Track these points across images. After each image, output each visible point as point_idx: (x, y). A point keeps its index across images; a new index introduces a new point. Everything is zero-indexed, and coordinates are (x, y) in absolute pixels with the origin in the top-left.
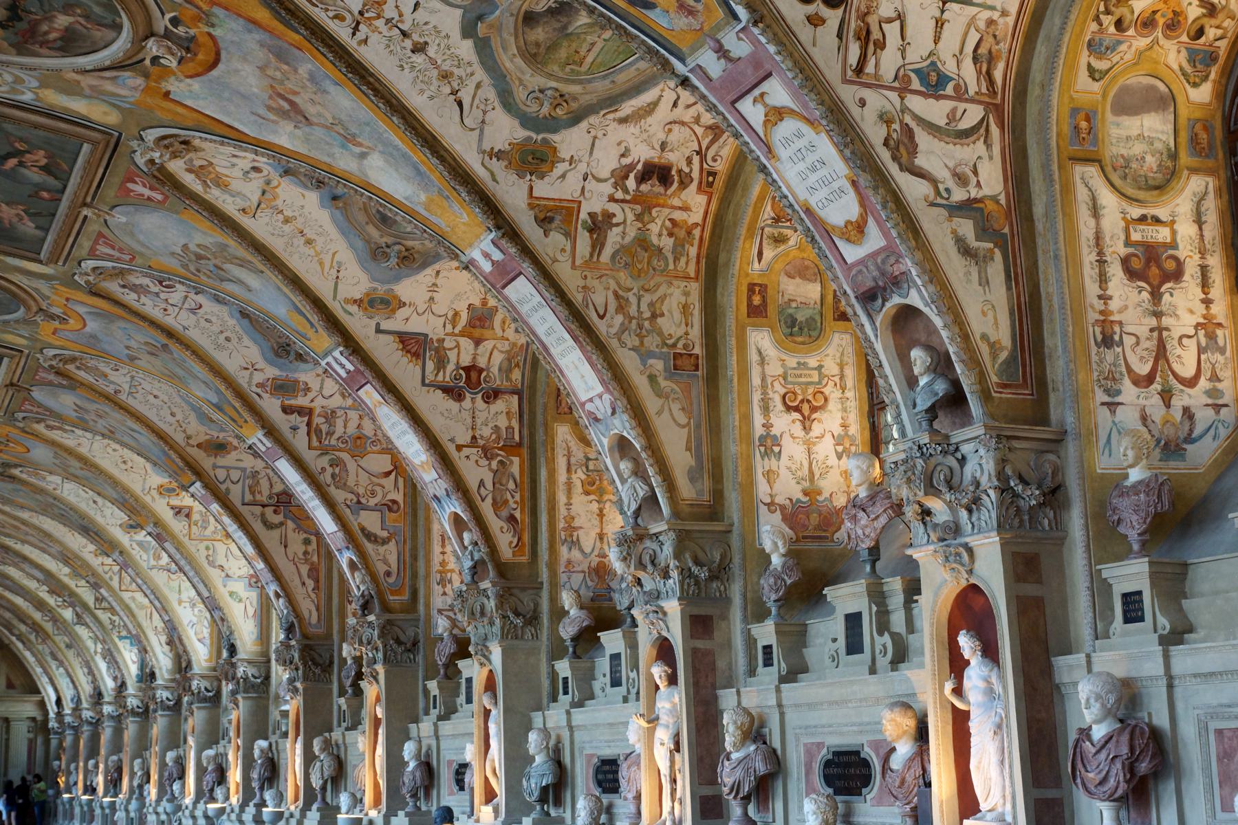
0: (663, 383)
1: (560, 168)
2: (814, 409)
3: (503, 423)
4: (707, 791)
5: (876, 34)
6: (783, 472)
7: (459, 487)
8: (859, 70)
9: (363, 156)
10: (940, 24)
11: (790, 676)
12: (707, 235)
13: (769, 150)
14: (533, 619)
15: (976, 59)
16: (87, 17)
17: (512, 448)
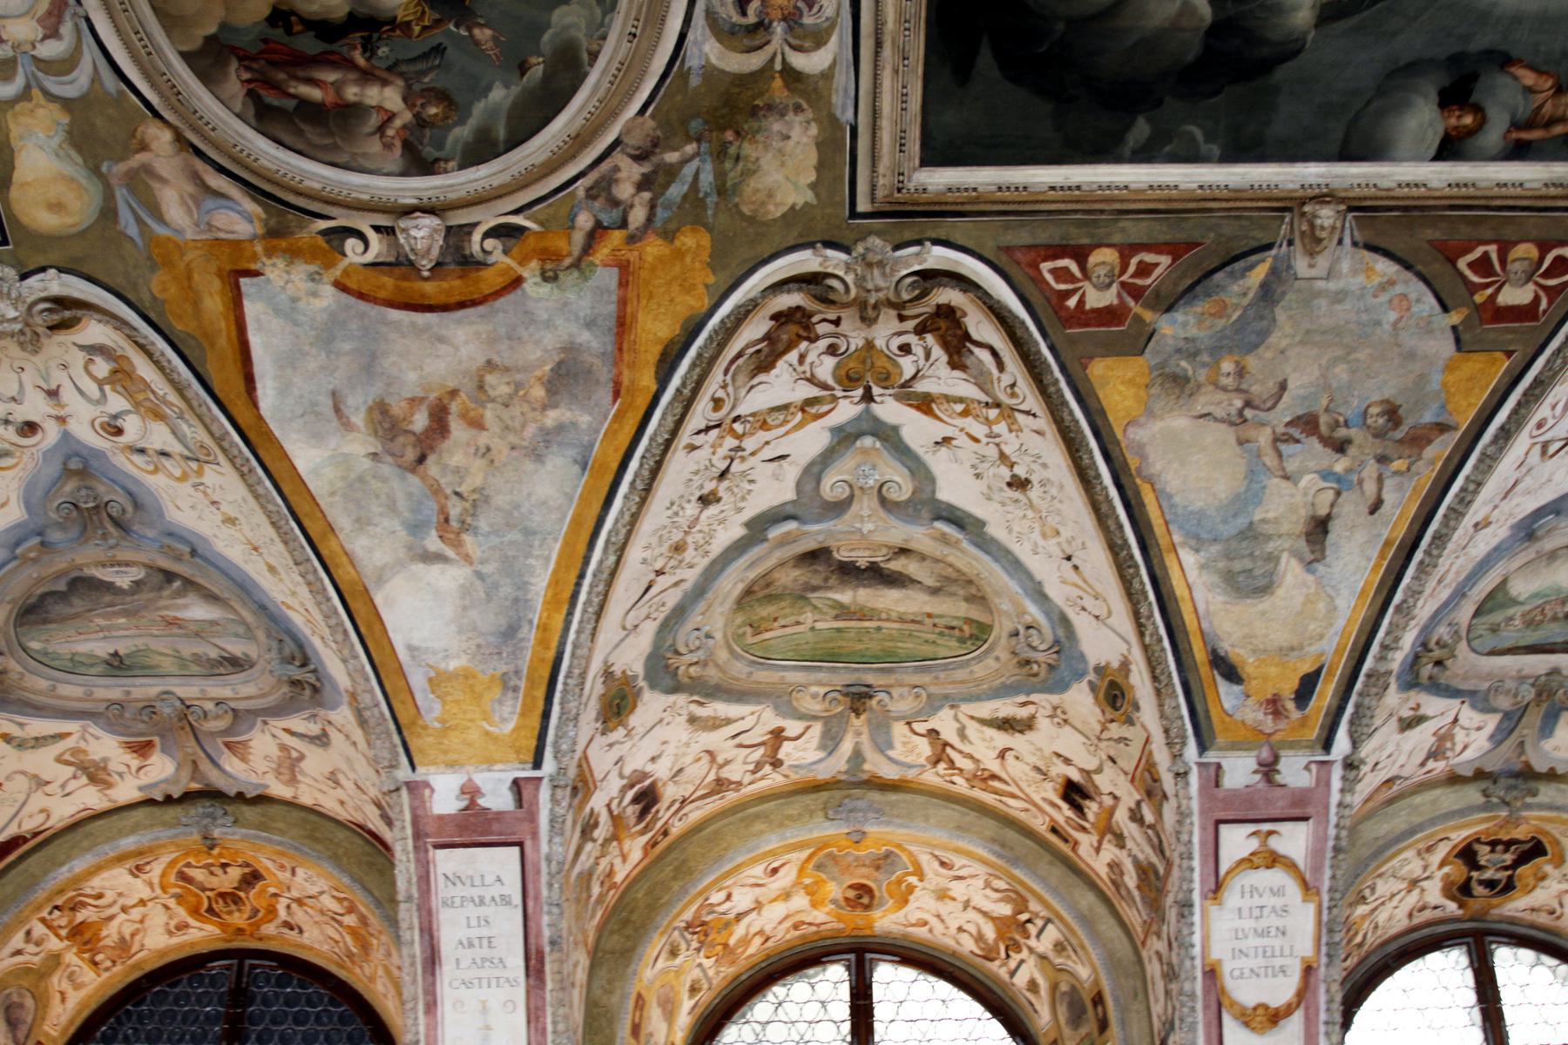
13: (1216, 888)
16: (421, 123)
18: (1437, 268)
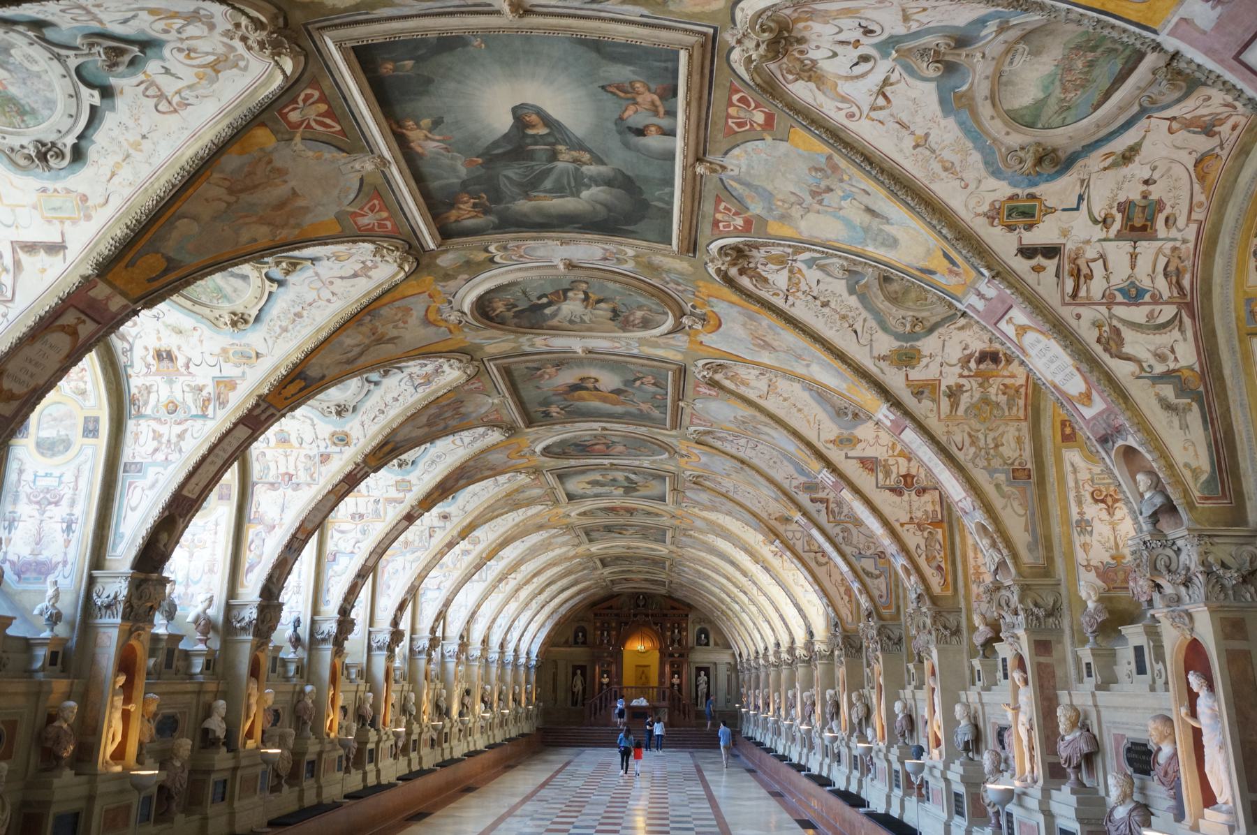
0: (1006, 489)
1: (924, 361)
2: (1116, 501)
3: (930, 508)
4: (1052, 759)
5: (1085, 270)
6: (1095, 543)
7: (904, 549)
8: (1075, 295)
9: (808, 366)
10: (1134, 257)
11: (1104, 686)
12: (1030, 391)
14: (957, 632)
15: (1166, 275)
17: (937, 524)
18: (739, 137)
